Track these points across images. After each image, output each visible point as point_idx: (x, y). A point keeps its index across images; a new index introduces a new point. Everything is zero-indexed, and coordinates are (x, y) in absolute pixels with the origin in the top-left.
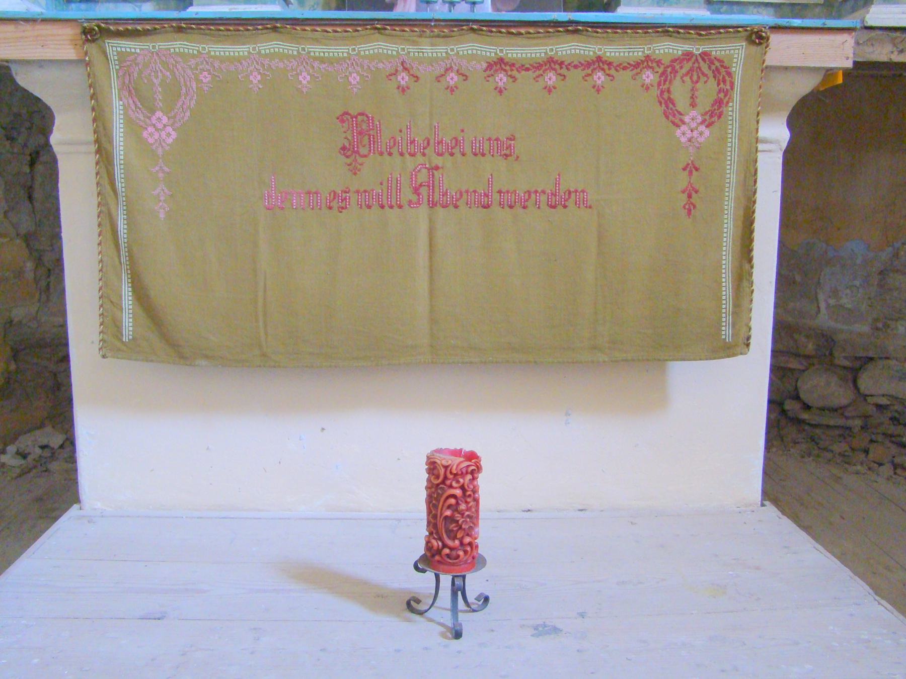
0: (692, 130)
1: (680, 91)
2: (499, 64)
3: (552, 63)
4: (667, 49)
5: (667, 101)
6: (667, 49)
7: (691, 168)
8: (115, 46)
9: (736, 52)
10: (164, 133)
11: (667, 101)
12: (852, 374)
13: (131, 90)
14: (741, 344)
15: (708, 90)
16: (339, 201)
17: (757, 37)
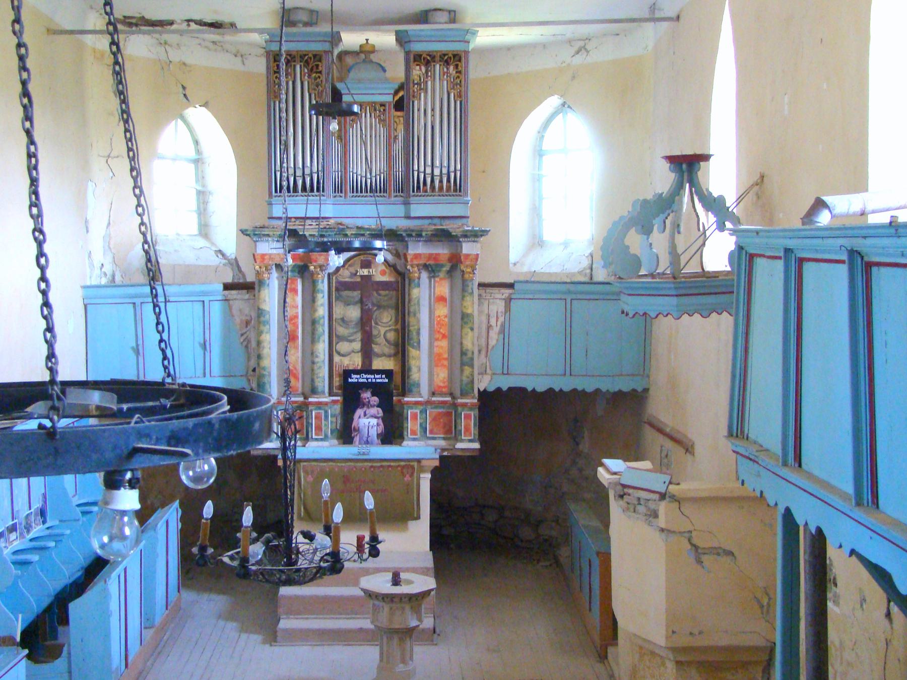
0: (407, 478)
1: (405, 471)
2: (372, 467)
3: (382, 466)
4: (402, 463)
5: (402, 472)
6: (402, 463)
7: (408, 485)
8: (302, 464)
9: (415, 464)
10: (310, 479)
11: (402, 472)
12: (538, 524)
13: (306, 472)
14: (418, 518)
15: (410, 471)
16: (343, 492)
17: (419, 461)
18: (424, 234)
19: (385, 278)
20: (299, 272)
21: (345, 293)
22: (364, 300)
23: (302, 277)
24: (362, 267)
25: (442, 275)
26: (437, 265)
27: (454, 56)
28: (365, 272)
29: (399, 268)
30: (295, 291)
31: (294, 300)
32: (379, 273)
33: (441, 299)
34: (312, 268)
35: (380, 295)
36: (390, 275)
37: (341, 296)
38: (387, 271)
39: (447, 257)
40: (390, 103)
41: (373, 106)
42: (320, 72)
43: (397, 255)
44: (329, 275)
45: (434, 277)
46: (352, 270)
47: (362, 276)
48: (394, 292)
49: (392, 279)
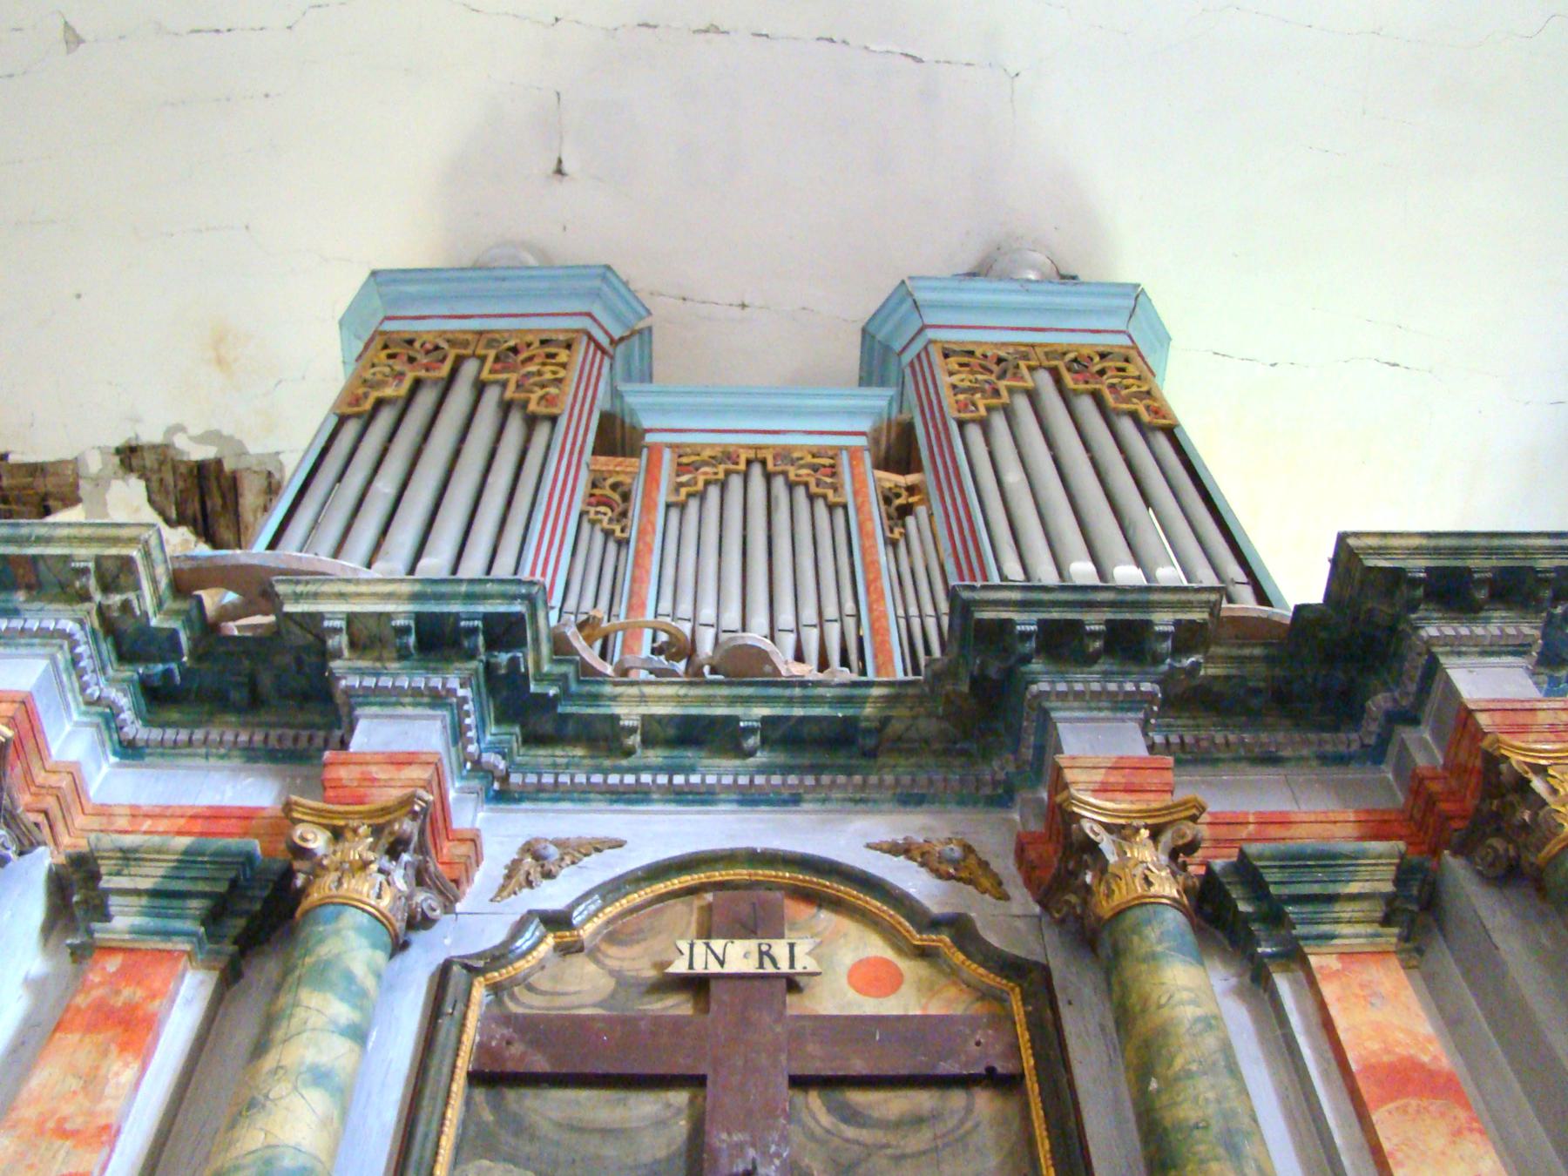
18: (1163, 620)
19: (903, 1003)
20: (214, 918)
21: (550, 1108)
22: (721, 1139)
23: (230, 977)
24: (706, 933)
25: (1352, 928)
26: (1296, 861)
27: (1103, 356)
28: (739, 956)
29: (993, 939)
30: (132, 1029)
31: (92, 1081)
32: (839, 968)
33: (1407, 1078)
34: (318, 841)
35: (852, 1116)
36: (930, 990)
37: (520, 1127)
38: (906, 966)
39: (1350, 830)
40: (854, 453)
41: (784, 454)
42: (564, 366)
43: (962, 867)
44: (445, 970)
45: (1294, 956)
46: (638, 962)
47: (697, 985)
48: (984, 1102)
49: (958, 1010)
